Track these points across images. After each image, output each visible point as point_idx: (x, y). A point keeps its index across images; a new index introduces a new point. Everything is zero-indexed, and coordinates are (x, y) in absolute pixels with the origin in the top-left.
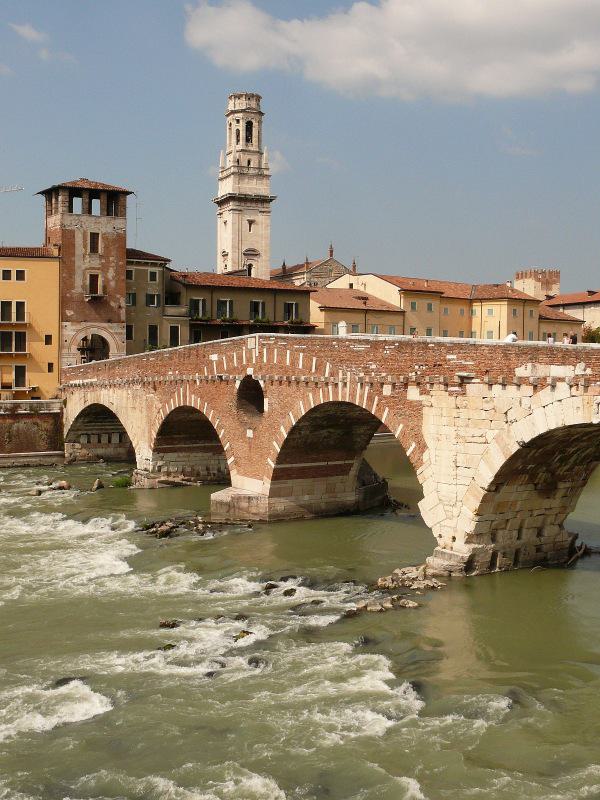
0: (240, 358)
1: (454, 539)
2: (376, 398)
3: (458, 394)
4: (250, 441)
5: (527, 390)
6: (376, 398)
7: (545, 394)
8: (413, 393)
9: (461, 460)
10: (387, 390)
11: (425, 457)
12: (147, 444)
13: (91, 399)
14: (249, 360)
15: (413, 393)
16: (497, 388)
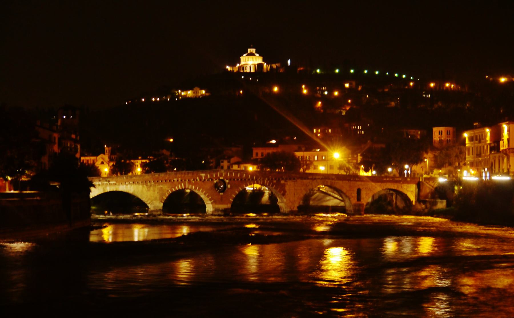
0: (216, 176)
1: (294, 208)
2: (271, 183)
3: (294, 182)
4: (222, 195)
5: (311, 181)
6: (271, 183)
7: (315, 181)
8: (282, 182)
9: (295, 193)
10: (275, 181)
11: (286, 194)
12: (159, 202)
13: (109, 189)
14: (221, 175)
15: (282, 182)
16: (305, 181)
